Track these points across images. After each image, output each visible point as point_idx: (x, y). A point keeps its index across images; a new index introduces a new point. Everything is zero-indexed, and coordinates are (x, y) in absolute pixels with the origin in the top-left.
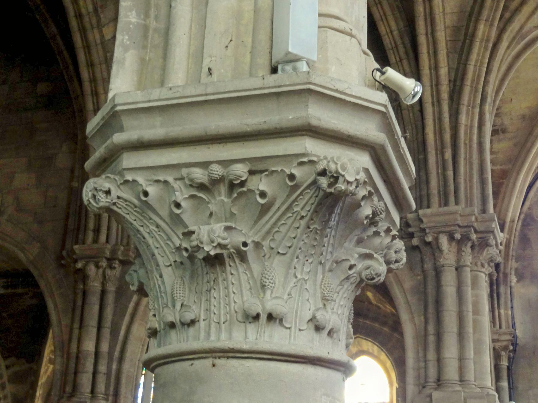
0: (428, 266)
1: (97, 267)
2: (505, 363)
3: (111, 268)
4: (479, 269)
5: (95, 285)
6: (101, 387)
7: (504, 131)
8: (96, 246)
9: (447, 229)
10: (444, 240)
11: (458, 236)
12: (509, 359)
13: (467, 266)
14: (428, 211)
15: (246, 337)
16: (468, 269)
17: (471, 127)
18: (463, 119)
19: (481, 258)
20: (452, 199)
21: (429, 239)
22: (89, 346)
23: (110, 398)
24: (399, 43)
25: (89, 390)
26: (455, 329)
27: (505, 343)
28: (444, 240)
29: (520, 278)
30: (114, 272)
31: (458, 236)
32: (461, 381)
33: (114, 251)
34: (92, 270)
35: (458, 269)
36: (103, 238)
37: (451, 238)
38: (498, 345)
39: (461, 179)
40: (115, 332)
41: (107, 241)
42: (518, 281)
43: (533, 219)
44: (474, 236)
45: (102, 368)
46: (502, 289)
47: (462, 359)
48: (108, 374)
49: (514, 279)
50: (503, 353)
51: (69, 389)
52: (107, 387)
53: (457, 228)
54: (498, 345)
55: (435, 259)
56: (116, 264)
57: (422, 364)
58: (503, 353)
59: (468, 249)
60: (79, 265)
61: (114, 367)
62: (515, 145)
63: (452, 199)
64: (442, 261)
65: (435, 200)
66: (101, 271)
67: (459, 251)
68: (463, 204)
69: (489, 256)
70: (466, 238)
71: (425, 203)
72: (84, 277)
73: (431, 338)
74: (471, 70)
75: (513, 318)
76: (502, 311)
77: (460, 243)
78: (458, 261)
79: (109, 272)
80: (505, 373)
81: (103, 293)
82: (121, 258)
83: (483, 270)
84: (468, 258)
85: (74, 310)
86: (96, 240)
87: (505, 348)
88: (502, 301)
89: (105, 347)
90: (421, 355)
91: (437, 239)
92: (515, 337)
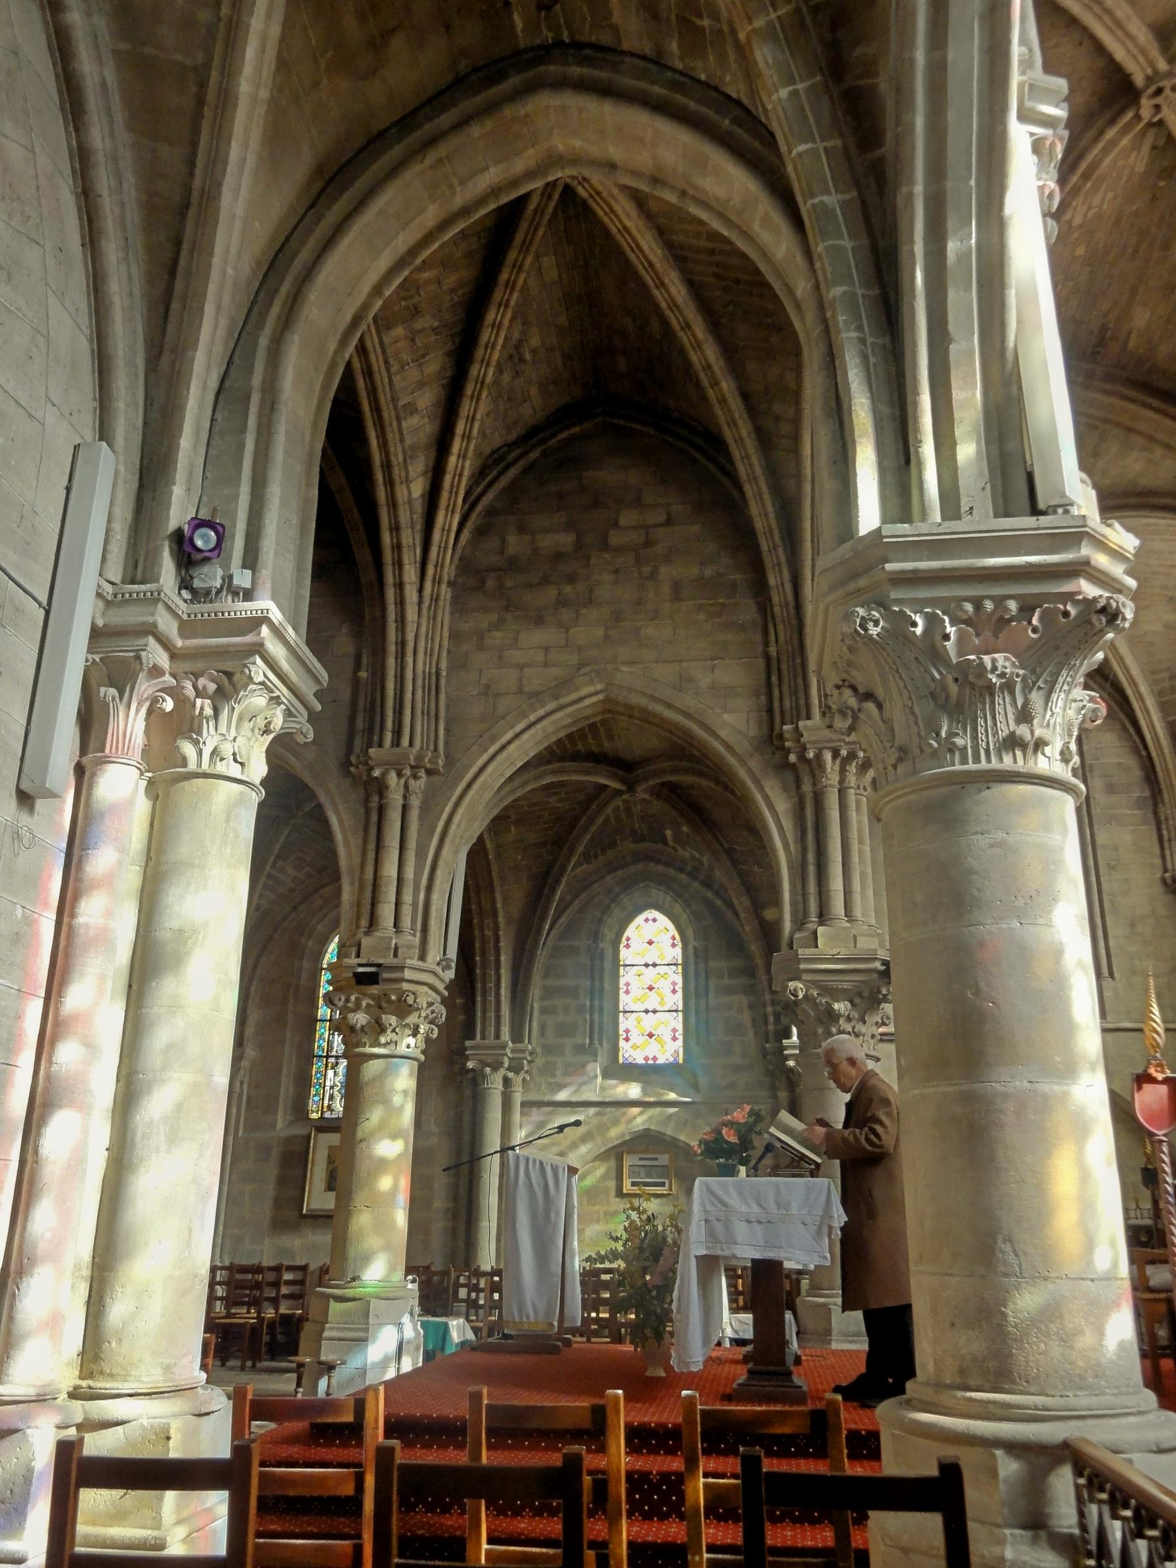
0: (807, 787)
1: (399, 775)
3: (415, 777)
5: (395, 797)
6: (406, 921)
8: (396, 750)
9: (833, 745)
10: (828, 756)
11: (844, 753)
14: (809, 723)
15: (1015, 761)
22: (390, 870)
23: (418, 934)
24: (774, 525)
25: (392, 923)
28: (828, 756)
30: (418, 782)
31: (844, 753)
33: (419, 758)
34: (392, 778)
35: (842, 792)
36: (405, 741)
37: (836, 754)
40: (421, 854)
41: (411, 744)
44: (861, 754)
45: (408, 897)
47: (847, 893)
48: (415, 905)
51: (364, 922)
52: (414, 921)
56: (422, 773)
57: (800, 898)
59: (853, 768)
60: (376, 773)
61: (422, 896)
66: (403, 781)
67: (843, 771)
70: (852, 756)
71: (803, 712)
72: (381, 787)
73: (811, 869)
77: (846, 761)
78: (841, 782)
79: (412, 782)
81: (405, 808)
82: (428, 766)
84: (852, 780)
85: (366, 829)
86: (396, 742)
89: (409, 873)
90: (799, 886)
91: (819, 756)
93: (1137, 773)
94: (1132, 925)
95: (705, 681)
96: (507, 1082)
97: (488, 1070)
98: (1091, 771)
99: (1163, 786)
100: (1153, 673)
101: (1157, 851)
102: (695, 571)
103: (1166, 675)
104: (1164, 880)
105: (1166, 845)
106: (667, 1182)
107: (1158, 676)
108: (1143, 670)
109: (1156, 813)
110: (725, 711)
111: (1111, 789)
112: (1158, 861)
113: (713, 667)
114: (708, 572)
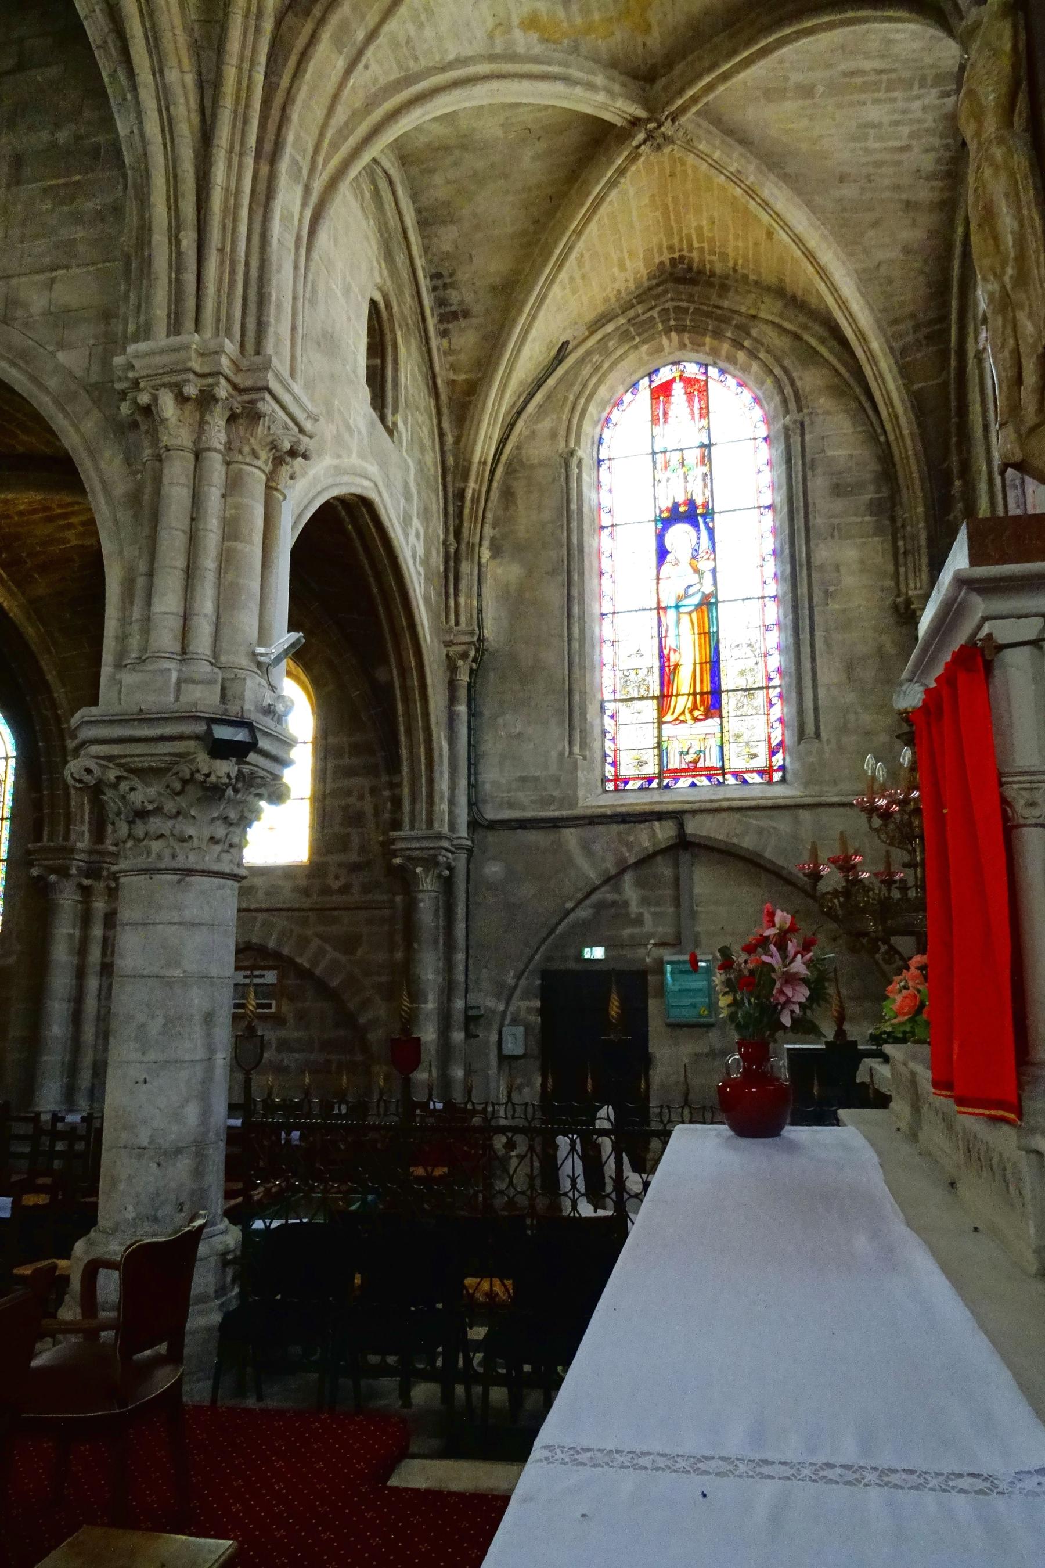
2: (464, 678)
4: (248, 460)
7: (466, 314)
9: (175, 379)
12: (472, 671)
13: (215, 450)
14: (143, 346)
16: (218, 457)
17: (238, 193)
18: (219, 175)
19: (252, 440)
20: (189, 324)
21: (144, 399)
26: (180, 562)
27: (460, 649)
29: (497, 550)
31: (191, 390)
32: (184, 652)
38: (453, 650)
39: (211, 288)
42: (493, 557)
43: (521, 463)
46: (465, 567)
49: (486, 554)
50: (460, 663)
53: (192, 376)
54: (453, 650)
55: (156, 441)
58: (460, 663)
59: (217, 421)
62: (485, 338)
63: (189, 324)
64: (165, 440)
65: (160, 327)
68: (208, 333)
69: (271, 438)
74: (230, 73)
75: (480, 611)
76: (462, 600)
80: (463, 694)
83: (260, 463)
84: (217, 433)
87: (464, 656)
88: (463, 584)
91: (155, 398)
92: (481, 640)
93: (874, 466)
94: (849, 668)
95: (37, 302)
96: (86, 892)
97: (53, 878)
98: (813, 467)
99: (901, 481)
100: (895, 322)
101: (890, 568)
102: (45, 136)
103: (910, 324)
104: (895, 607)
105: (901, 560)
106: (274, 1002)
107: (901, 327)
108: (878, 321)
109: (893, 519)
110: (61, 346)
111: (838, 490)
112: (890, 583)
113: (53, 281)
114: (63, 136)
